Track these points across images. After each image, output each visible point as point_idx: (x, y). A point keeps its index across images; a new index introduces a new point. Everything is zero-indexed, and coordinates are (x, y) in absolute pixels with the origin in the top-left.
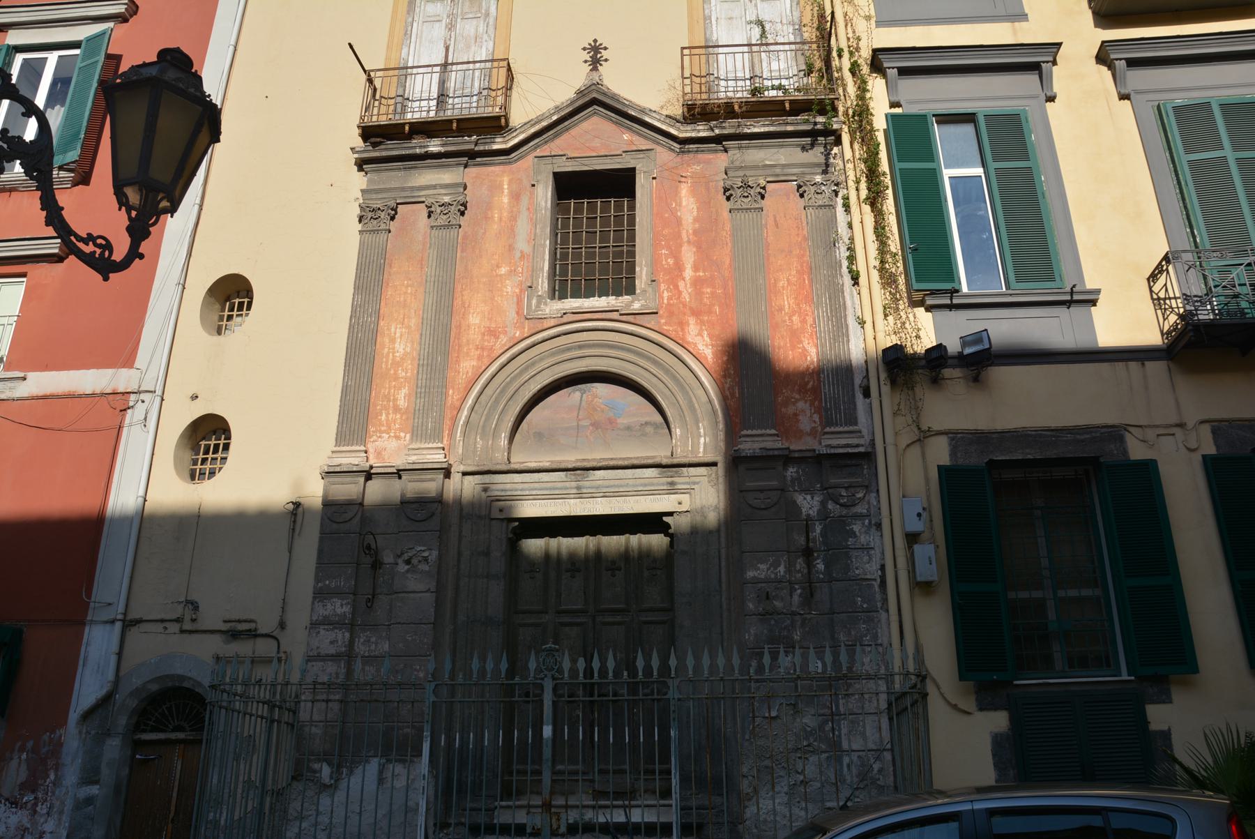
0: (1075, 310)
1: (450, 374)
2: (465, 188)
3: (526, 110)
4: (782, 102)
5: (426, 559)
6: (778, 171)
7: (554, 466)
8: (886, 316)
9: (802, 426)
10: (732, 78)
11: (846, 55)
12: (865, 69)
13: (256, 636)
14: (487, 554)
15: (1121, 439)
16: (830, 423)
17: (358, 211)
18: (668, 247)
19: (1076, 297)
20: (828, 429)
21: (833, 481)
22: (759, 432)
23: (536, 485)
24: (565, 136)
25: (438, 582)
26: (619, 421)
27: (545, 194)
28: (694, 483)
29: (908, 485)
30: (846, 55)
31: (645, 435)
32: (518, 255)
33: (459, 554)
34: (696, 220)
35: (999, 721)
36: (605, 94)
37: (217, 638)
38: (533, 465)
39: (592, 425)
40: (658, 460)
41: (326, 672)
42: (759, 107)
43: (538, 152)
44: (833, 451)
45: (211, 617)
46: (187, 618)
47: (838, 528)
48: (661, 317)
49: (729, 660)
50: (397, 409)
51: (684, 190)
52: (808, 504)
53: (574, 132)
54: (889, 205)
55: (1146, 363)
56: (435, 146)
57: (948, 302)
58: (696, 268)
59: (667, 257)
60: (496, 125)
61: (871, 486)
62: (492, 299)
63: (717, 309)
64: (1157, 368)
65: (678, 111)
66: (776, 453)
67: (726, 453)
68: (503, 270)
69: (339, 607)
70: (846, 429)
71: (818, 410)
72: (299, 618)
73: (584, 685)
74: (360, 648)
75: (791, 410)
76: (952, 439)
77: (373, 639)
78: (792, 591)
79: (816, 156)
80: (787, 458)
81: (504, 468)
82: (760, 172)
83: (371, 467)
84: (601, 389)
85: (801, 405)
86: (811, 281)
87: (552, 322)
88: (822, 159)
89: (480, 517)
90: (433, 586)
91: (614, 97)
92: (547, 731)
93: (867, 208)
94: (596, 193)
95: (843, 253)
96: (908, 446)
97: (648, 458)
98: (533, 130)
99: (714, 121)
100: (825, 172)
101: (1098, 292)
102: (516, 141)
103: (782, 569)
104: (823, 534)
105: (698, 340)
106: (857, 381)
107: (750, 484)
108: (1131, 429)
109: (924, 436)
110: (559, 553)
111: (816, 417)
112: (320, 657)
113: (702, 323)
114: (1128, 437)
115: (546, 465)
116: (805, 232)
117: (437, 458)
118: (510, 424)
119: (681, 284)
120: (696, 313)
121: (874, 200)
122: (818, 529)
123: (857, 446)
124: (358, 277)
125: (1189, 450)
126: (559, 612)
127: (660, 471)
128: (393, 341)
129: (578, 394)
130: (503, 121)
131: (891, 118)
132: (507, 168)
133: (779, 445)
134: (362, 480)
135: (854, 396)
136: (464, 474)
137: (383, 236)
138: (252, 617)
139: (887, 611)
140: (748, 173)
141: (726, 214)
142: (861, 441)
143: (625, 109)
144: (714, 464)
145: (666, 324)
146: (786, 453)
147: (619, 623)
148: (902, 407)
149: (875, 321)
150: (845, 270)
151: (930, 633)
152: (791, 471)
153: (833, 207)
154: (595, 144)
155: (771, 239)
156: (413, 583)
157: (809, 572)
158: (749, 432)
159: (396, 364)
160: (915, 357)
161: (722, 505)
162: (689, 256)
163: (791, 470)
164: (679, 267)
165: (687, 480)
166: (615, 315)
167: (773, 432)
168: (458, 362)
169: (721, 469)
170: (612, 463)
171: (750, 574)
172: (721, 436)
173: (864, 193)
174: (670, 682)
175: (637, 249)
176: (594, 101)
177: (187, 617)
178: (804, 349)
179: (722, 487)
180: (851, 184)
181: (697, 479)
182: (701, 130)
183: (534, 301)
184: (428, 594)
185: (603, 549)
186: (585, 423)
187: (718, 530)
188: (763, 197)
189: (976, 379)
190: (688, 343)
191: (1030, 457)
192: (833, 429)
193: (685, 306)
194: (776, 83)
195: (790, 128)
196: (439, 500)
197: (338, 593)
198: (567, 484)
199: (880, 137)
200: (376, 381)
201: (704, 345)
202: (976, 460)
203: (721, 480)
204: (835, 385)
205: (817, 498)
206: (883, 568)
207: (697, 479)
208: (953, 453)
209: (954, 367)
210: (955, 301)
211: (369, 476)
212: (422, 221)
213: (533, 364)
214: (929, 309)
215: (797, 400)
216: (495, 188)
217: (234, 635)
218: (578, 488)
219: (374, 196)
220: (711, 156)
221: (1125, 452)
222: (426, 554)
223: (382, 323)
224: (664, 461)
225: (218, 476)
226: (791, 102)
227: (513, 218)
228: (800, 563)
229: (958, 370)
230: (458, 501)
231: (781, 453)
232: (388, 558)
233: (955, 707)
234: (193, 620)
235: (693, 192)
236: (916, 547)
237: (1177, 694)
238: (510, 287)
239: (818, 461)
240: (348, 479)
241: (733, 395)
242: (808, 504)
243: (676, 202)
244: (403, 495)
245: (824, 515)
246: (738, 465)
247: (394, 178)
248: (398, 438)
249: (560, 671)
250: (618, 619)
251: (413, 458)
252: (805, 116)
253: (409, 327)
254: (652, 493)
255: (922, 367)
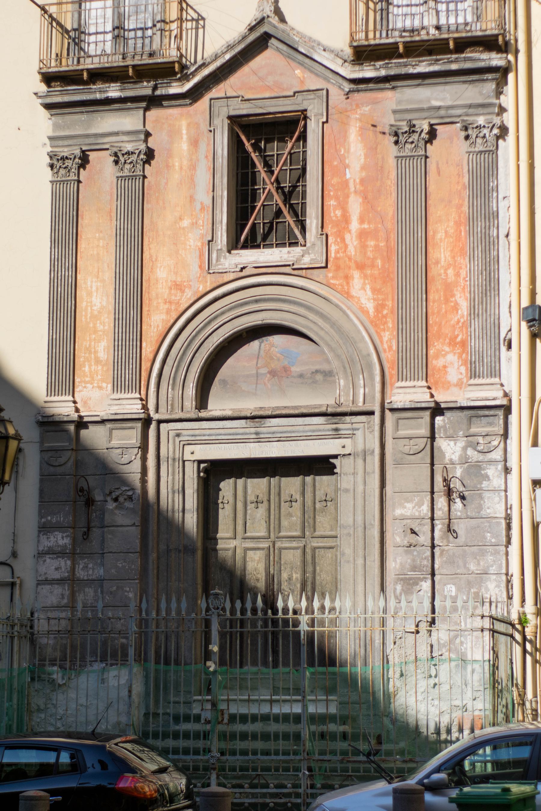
6: (442, 112)
7: (236, 415)
16: (474, 374)
17: (48, 160)
18: (337, 198)
22: (412, 383)
26: (293, 369)
31: (315, 382)
32: (199, 206)
34: (363, 168)
39: (270, 372)
50: (98, 361)
56: (114, 91)
58: (362, 221)
63: (379, 262)
68: (186, 223)
71: (465, 363)
72: (27, 550)
77: (90, 566)
82: (425, 114)
84: (278, 339)
87: (232, 276)
90: (137, 520)
111: (463, 369)
113: (365, 277)
115: (229, 413)
116: (466, 180)
117: (134, 408)
119: (347, 237)
120: (360, 267)
128: (90, 294)
141: (392, 162)
145: (333, 278)
156: (121, 518)
162: (355, 206)
164: (346, 219)
165: (349, 426)
166: (287, 270)
170: (284, 412)
174: (301, 618)
181: (355, 426)
182: (368, 72)
184: (134, 528)
186: (263, 371)
193: (350, 259)
195: (454, 67)
197: (59, 527)
198: (247, 430)
207: (355, 426)
213: (215, 318)
215: (447, 353)
216: (174, 133)
219: (61, 143)
224: (330, 410)
227: (193, 167)
232: (98, 497)
245: (464, 460)
247: (80, 124)
248: (100, 388)
249: (224, 609)
250: (294, 544)
253: (103, 281)
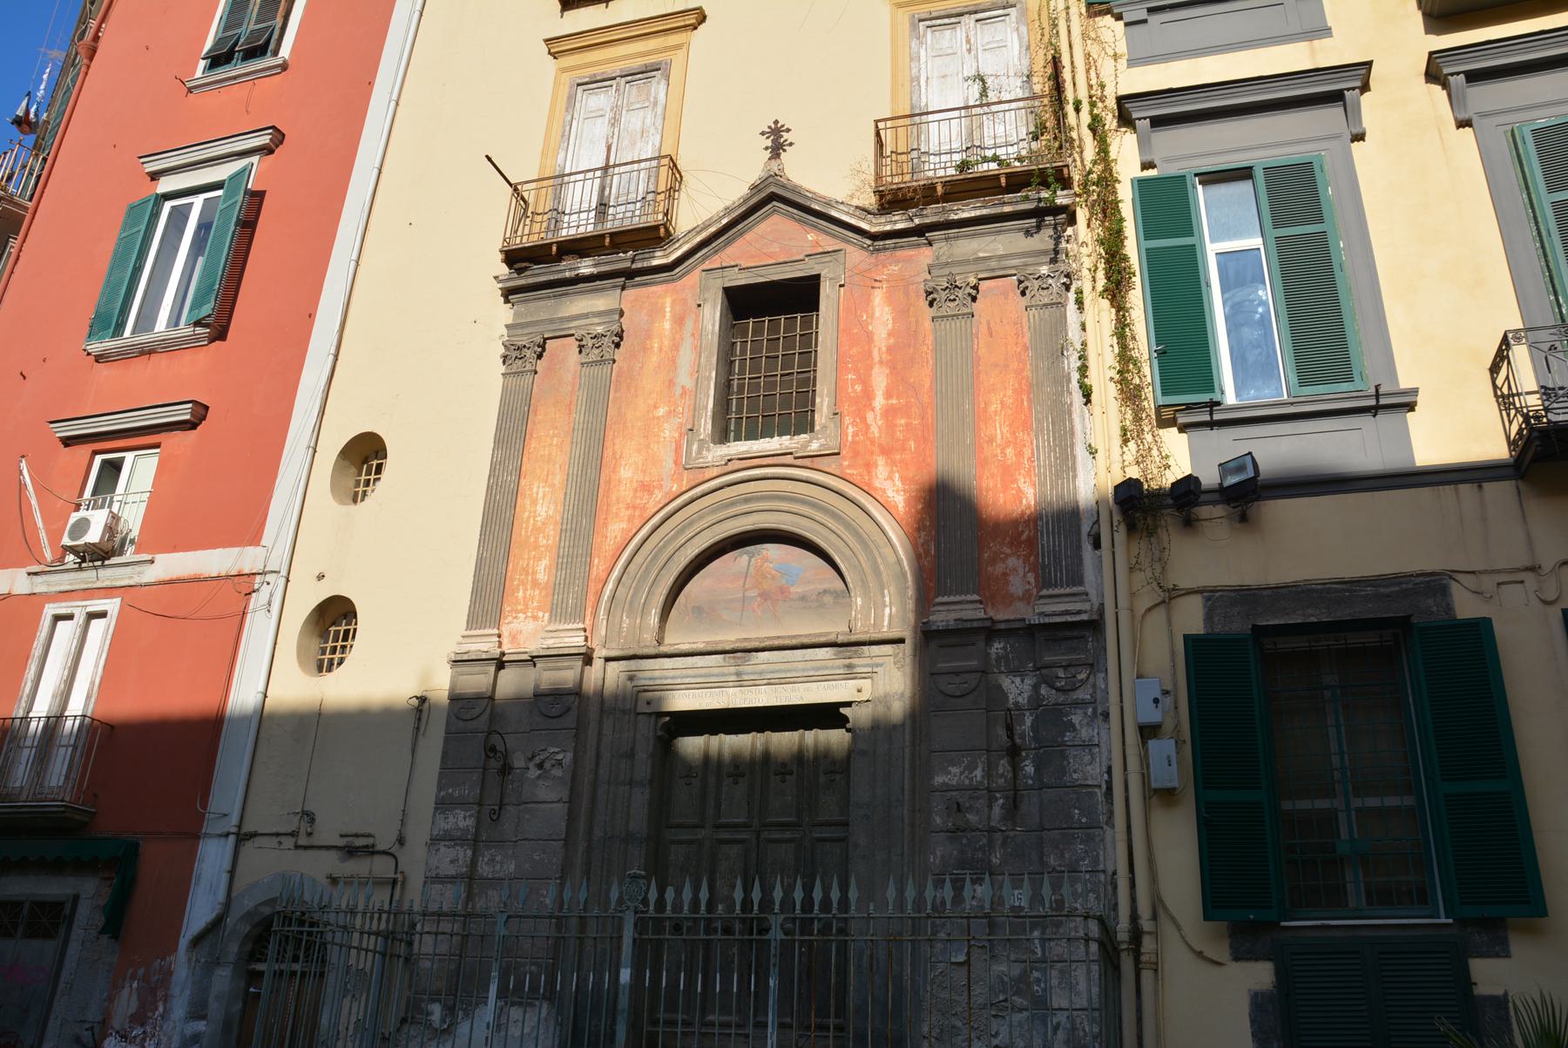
0: (1382, 417)
1: (597, 539)
2: (622, 314)
3: (693, 214)
4: (997, 177)
5: (559, 763)
6: (993, 264)
7: (710, 648)
8: (1125, 442)
9: (1012, 589)
10: (941, 150)
11: (1085, 108)
12: (1110, 122)
13: (373, 853)
14: (631, 755)
15: (1444, 591)
16: (1045, 582)
17: (502, 350)
18: (856, 371)
19: (1383, 401)
20: (1044, 592)
21: (1048, 659)
22: (958, 598)
23: (690, 672)
24: (739, 243)
25: (572, 789)
26: (792, 590)
27: (712, 315)
28: (878, 665)
29: (1145, 666)
30: (1085, 108)
31: (823, 606)
32: (679, 391)
33: (598, 756)
34: (890, 334)
35: (1261, 975)
36: (784, 187)
37: (333, 854)
38: (685, 647)
39: (761, 595)
40: (832, 638)
41: (448, 897)
42: (965, 187)
43: (707, 265)
44: (1047, 620)
45: (327, 832)
46: (303, 831)
47: (1052, 718)
48: (844, 458)
49: (901, 891)
50: (535, 584)
51: (878, 297)
52: (1017, 689)
53: (749, 236)
54: (1137, 298)
55: (1485, 485)
56: (586, 267)
57: (1207, 418)
58: (888, 395)
59: (854, 382)
60: (654, 236)
61: (1095, 665)
62: (648, 446)
63: (912, 444)
64: (1501, 492)
65: (870, 200)
66: (975, 624)
67: (915, 627)
68: (661, 412)
69: (462, 820)
70: (1068, 590)
71: (1034, 569)
72: (419, 834)
73: (743, 921)
74: (484, 869)
75: (999, 569)
76: (1208, 599)
77: (498, 858)
78: (991, 801)
79: (1042, 241)
80: (990, 631)
81: (652, 651)
82: (972, 268)
83: (503, 654)
84: (773, 551)
85: (1012, 562)
86: (1029, 400)
87: (715, 472)
88: (1051, 245)
89: (624, 712)
90: (565, 795)
91: (795, 190)
92: (625, 975)
93: (1106, 303)
94: (773, 308)
95: (1073, 363)
96: (1149, 610)
97: (821, 635)
98: (699, 239)
99: (915, 208)
100: (1054, 261)
101: (1415, 391)
102: (679, 253)
103: (978, 773)
104: (1034, 727)
105: (887, 485)
106: (1085, 529)
107: (943, 666)
108: (1459, 577)
109: (1171, 596)
110: (720, 754)
111: (1031, 577)
112: (438, 879)
113: (893, 463)
114: (1455, 588)
115: (701, 646)
116: (1027, 340)
117: (576, 641)
118: (662, 598)
119: (870, 416)
120: (886, 451)
121: (1116, 290)
122: (1028, 721)
123: (1079, 612)
124: (499, 428)
125: (1545, 602)
126: (718, 827)
127: (827, 647)
128: (534, 502)
129: (745, 558)
130: (662, 230)
131: (1141, 185)
132: (671, 286)
133: (981, 615)
134: (492, 669)
135: (1079, 547)
136: (608, 660)
137: (529, 377)
138: (368, 831)
139: (1113, 826)
140: (955, 270)
141: (928, 324)
142: (1086, 606)
143: (808, 203)
144: (901, 641)
145: (849, 466)
146: (988, 624)
147: (789, 841)
148: (1142, 559)
149: (1106, 452)
150: (1074, 385)
151: (1173, 856)
152: (997, 647)
153: (1061, 305)
154: (774, 249)
155: (982, 351)
156: (545, 791)
157: (1015, 777)
158: (946, 599)
159: (537, 530)
160: (1158, 494)
161: (908, 693)
162: (880, 380)
163: (996, 645)
164: (868, 395)
165: (868, 661)
166: (789, 459)
167: (976, 597)
168: (605, 525)
169: (907, 647)
170: (776, 643)
171: (939, 779)
172: (911, 605)
173: (1101, 282)
174: (772, 919)
175: (819, 374)
176: (771, 197)
177: (301, 832)
178: (1020, 490)
179: (908, 669)
180: (1085, 272)
181: (876, 660)
182: (899, 222)
183: (695, 447)
184: (559, 805)
185: (772, 749)
186: (753, 593)
187: (903, 725)
188: (974, 299)
189: (1243, 518)
190: (875, 489)
191: (1313, 619)
192: (1051, 592)
193: (873, 442)
194: (989, 153)
195: (1007, 209)
196: (577, 692)
197: (462, 804)
198: (725, 670)
199: (1127, 210)
200: (514, 550)
201: (894, 489)
202: (1239, 626)
203: (908, 660)
204: (1057, 534)
205: (1029, 681)
206: (1109, 771)
207: (876, 660)
208: (1209, 618)
209: (1214, 503)
210: (1216, 417)
211: (500, 664)
212: (573, 357)
213: (691, 524)
214: (1183, 429)
215: (1007, 556)
216: (656, 312)
217: (351, 852)
218: (738, 674)
219: (520, 331)
220: (912, 252)
221: (1449, 608)
222: (560, 757)
223: (523, 482)
224: (841, 639)
225: (337, 672)
226: (1008, 175)
227: (676, 347)
228: (1003, 766)
229: (1220, 507)
230: (600, 694)
231: (980, 624)
232: (518, 762)
233: (1200, 954)
234: (310, 834)
235: (889, 299)
236: (1151, 743)
237: (1517, 944)
238: (669, 432)
239: (1031, 632)
240: (478, 669)
241: (927, 552)
242: (1017, 689)
243: (868, 314)
244: (537, 686)
245: (1036, 702)
246: (932, 642)
247: (545, 309)
248: (535, 618)
249: (645, 902)
250: (788, 835)
251: (550, 642)
252: (1029, 194)
253: (553, 486)
254: (826, 678)
255: (1168, 506)
